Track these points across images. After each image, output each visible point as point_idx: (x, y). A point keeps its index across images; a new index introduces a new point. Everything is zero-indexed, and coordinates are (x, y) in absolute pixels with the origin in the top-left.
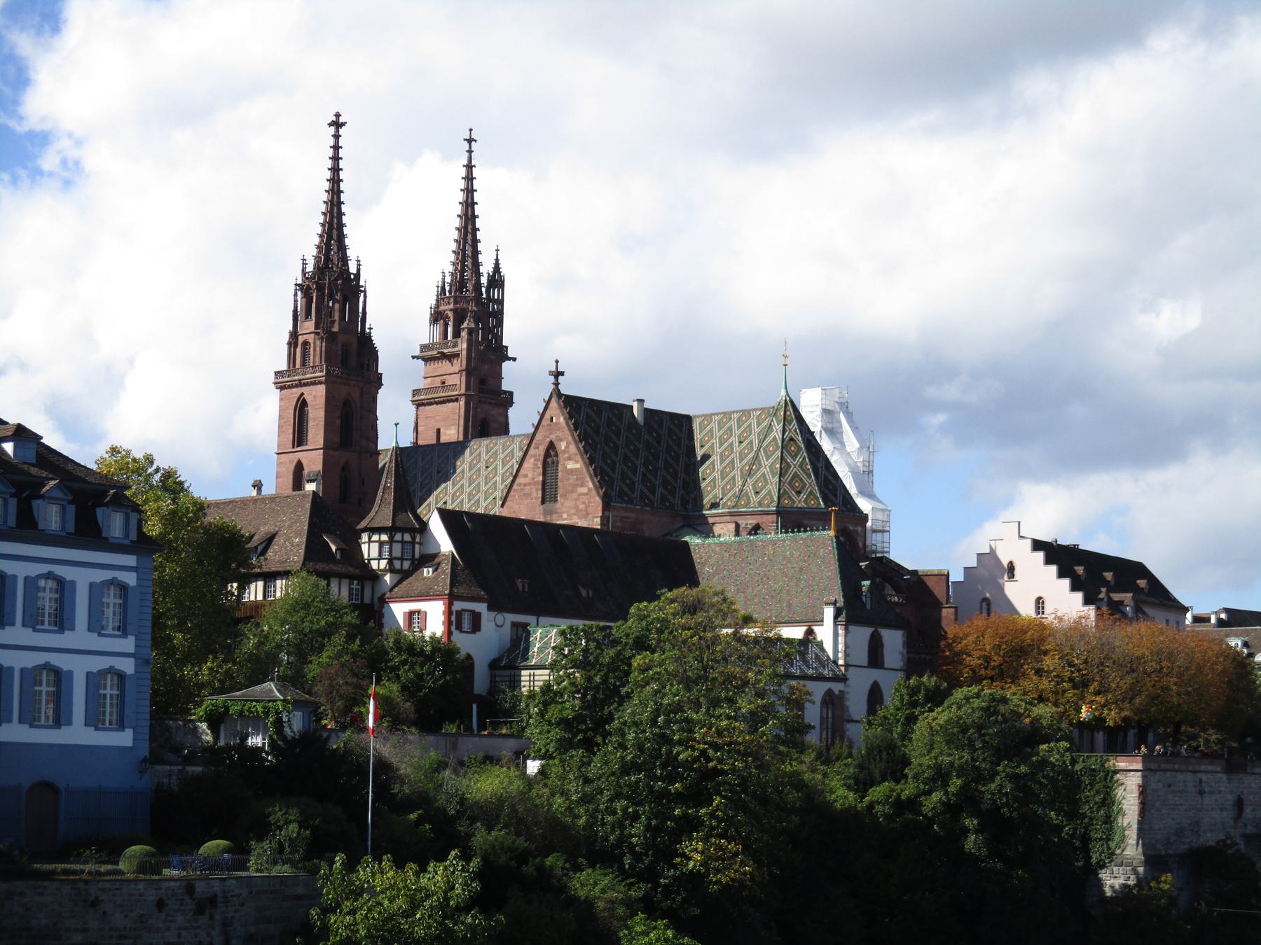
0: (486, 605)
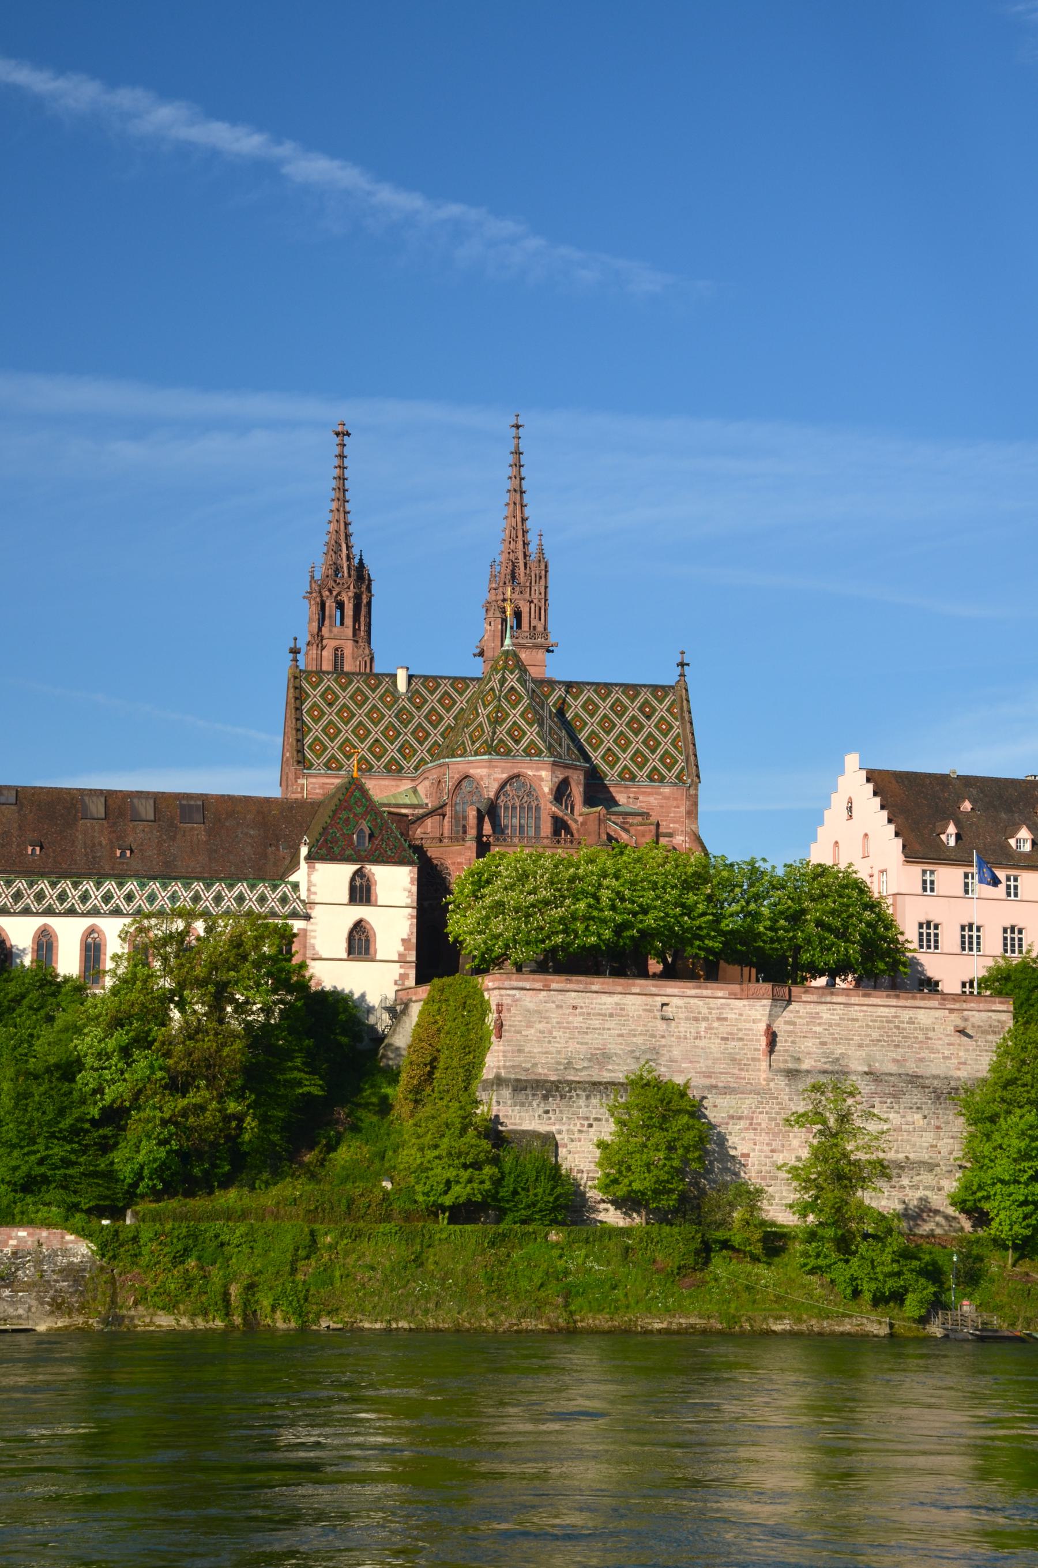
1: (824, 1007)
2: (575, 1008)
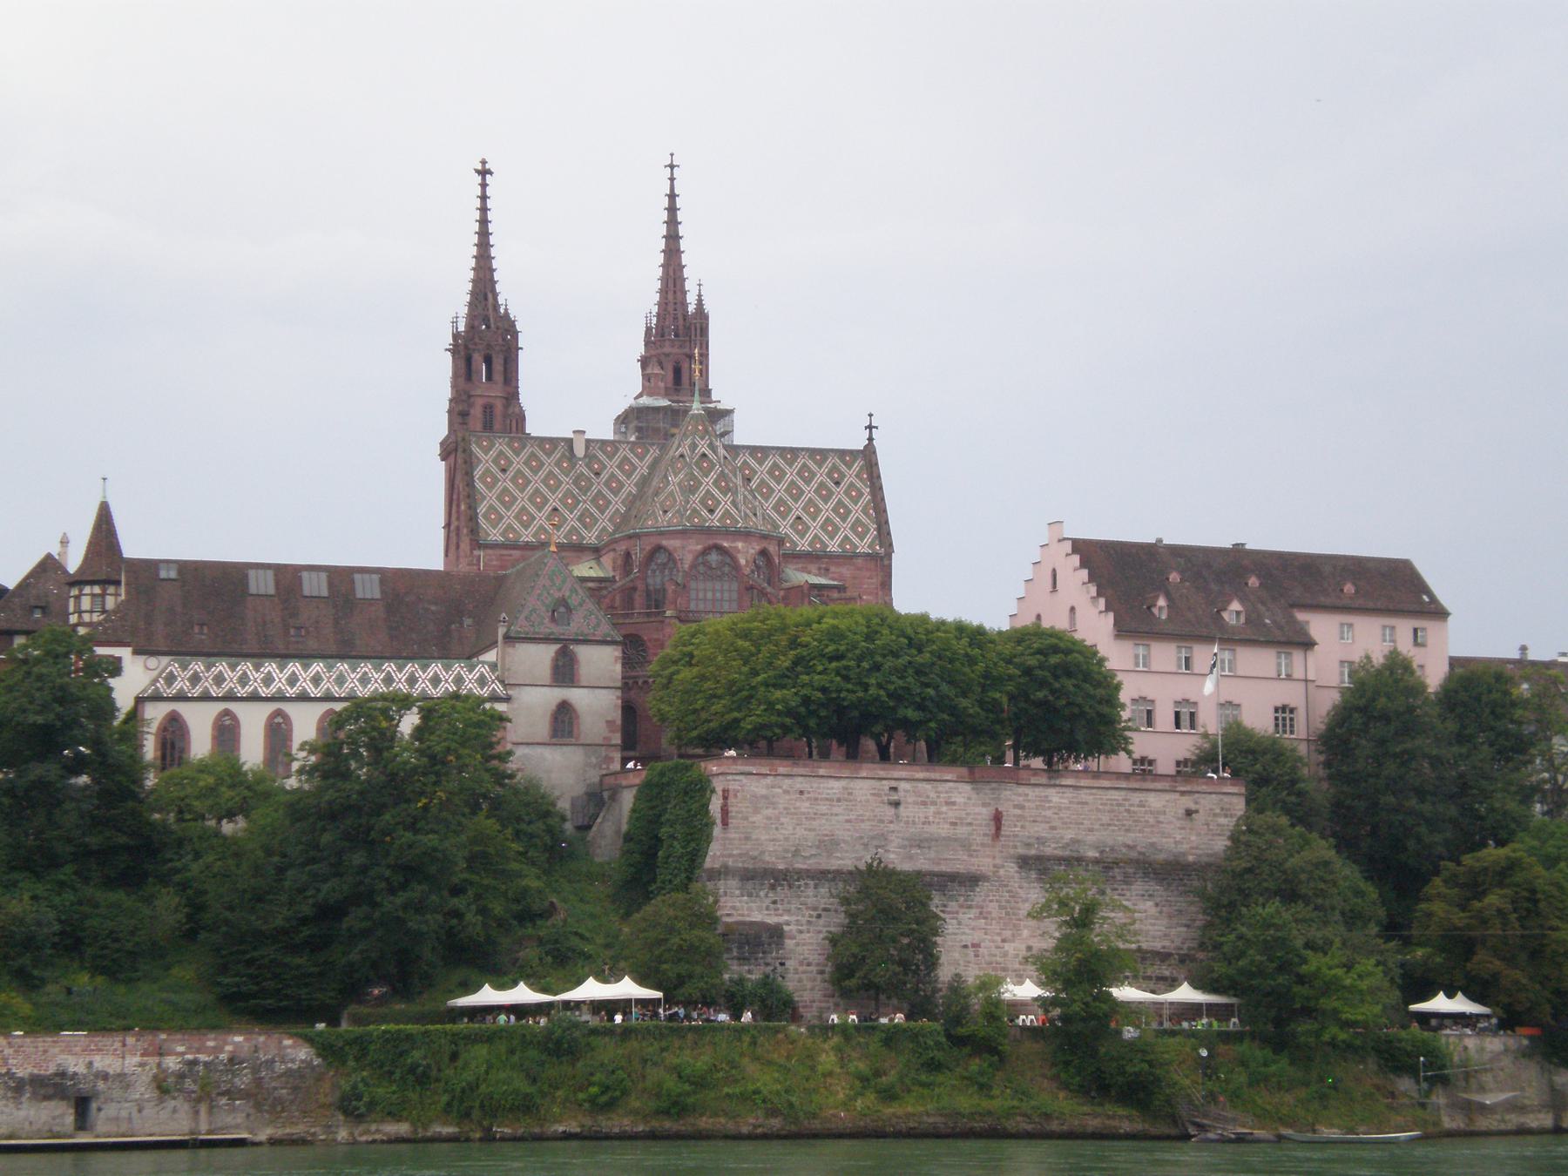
0: (129, 650)
1: (1051, 792)
2: (801, 792)
